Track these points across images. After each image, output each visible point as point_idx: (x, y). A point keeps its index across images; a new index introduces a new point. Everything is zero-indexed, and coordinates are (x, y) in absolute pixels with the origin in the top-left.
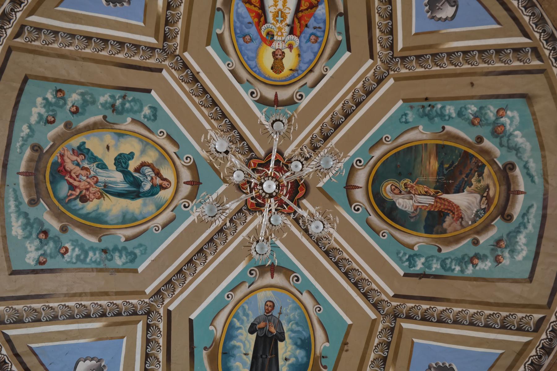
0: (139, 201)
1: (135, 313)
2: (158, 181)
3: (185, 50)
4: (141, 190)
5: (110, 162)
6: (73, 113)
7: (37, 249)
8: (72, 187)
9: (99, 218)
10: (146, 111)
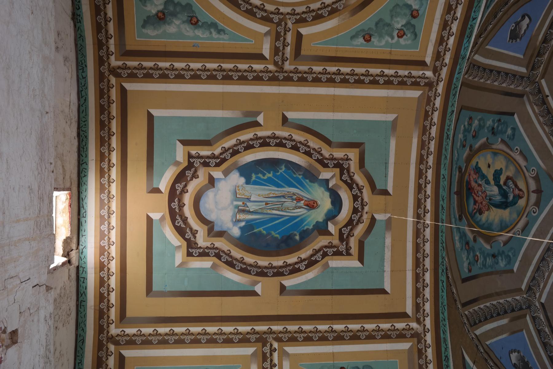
0: (508, 211)
1: (521, 309)
2: (517, 192)
3: (543, 77)
4: (508, 201)
5: (491, 178)
6: (474, 137)
7: (467, 259)
8: (475, 202)
9: (489, 227)
10: (509, 132)
